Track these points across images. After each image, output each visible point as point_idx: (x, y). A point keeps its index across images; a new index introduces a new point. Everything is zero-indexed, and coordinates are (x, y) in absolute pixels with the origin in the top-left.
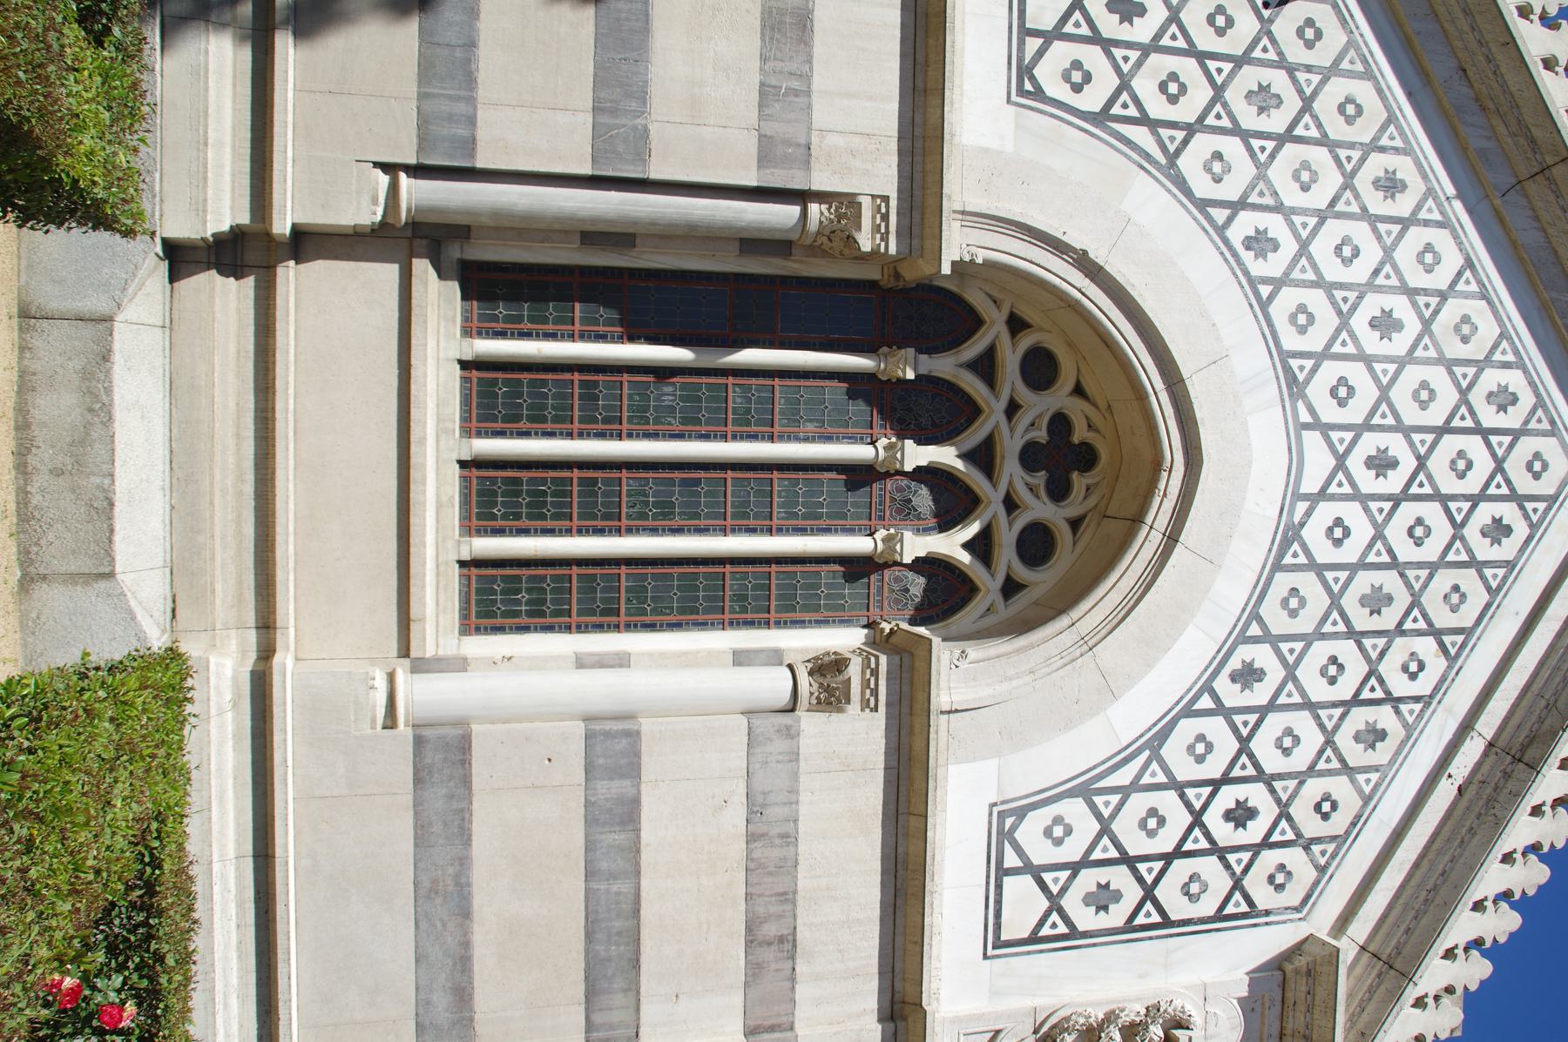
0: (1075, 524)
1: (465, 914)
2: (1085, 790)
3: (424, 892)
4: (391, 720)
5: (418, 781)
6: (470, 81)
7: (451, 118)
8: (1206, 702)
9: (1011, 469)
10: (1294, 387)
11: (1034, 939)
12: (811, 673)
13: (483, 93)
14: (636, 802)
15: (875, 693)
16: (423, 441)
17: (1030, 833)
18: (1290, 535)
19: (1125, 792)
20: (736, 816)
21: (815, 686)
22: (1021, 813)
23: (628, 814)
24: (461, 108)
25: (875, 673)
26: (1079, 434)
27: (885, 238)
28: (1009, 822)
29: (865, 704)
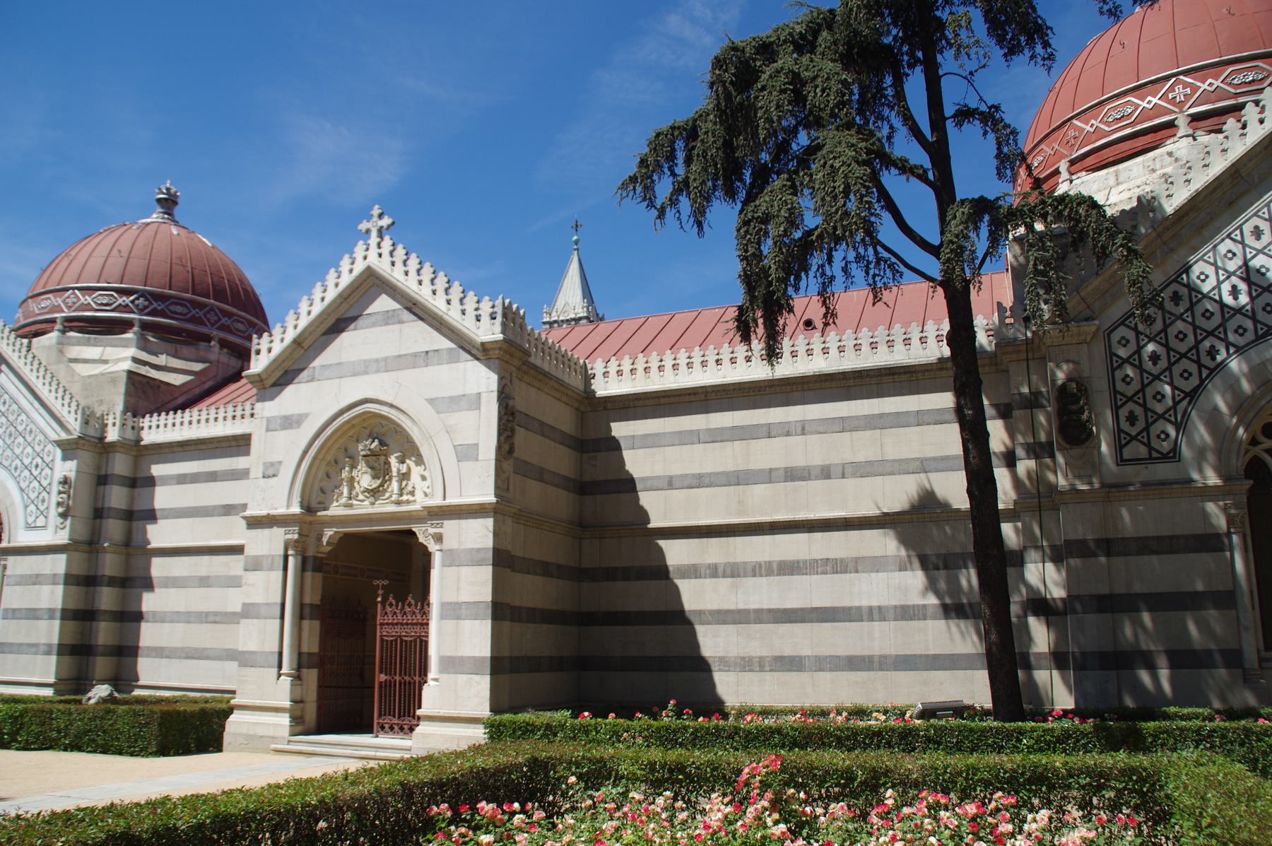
1: (21, 644)
2: (26, 507)
3: (19, 652)
17: (30, 520)
20: (17, 588)
23: (14, 610)
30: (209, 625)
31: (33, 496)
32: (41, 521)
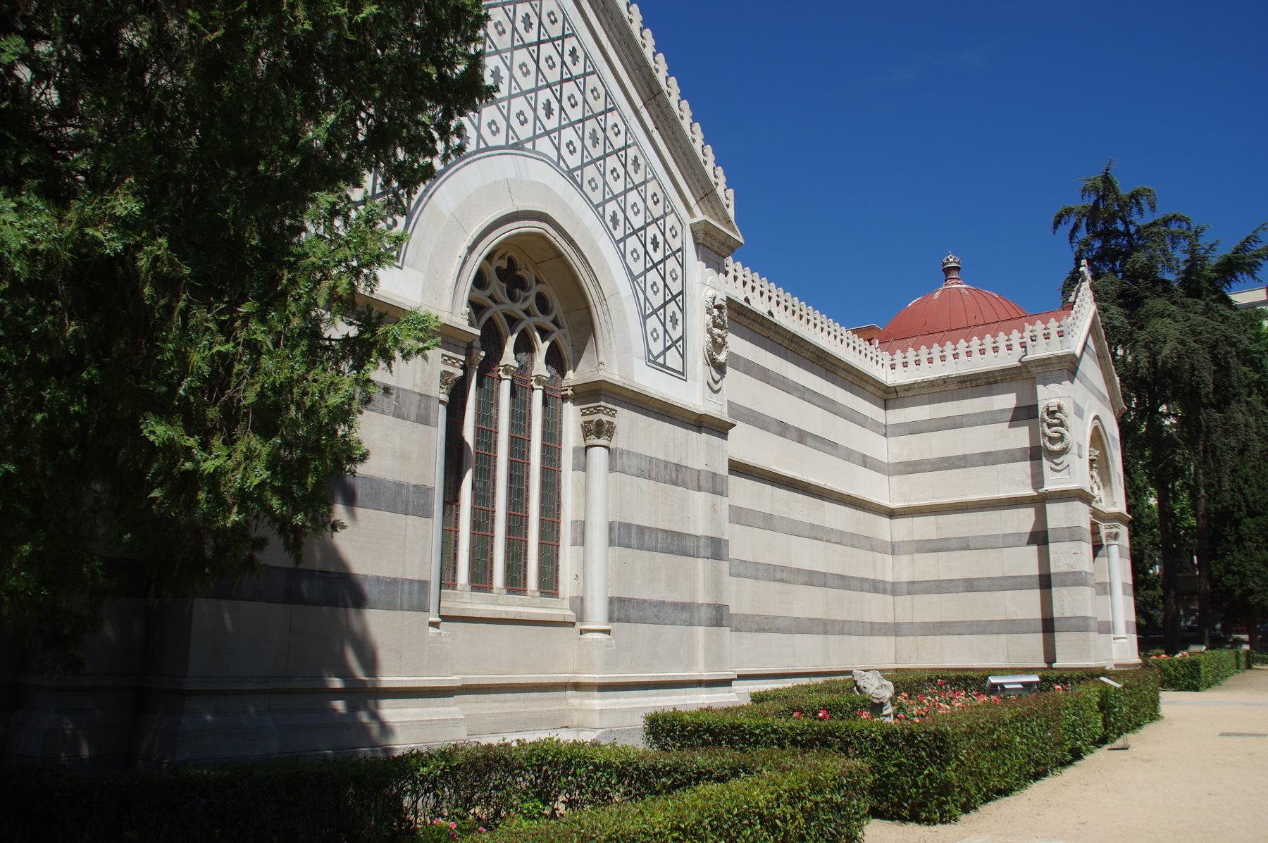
0: (538, 282)
2: (645, 317)
3: (658, 621)
4: (608, 632)
5: (628, 621)
6: (393, 582)
7: (410, 593)
8: (621, 245)
9: (517, 308)
10: (518, 146)
11: (682, 356)
12: (599, 438)
13: (399, 576)
14: (638, 527)
15: (611, 410)
16: (507, 612)
18: (570, 174)
19: (646, 298)
20: (644, 482)
21: (605, 437)
22: (649, 351)
23: (641, 529)
24: (406, 587)
25: (606, 408)
26: (504, 264)
27: (458, 360)
28: (651, 358)
29: (613, 416)
30: (777, 584)
31: (657, 301)
32: (673, 359)
